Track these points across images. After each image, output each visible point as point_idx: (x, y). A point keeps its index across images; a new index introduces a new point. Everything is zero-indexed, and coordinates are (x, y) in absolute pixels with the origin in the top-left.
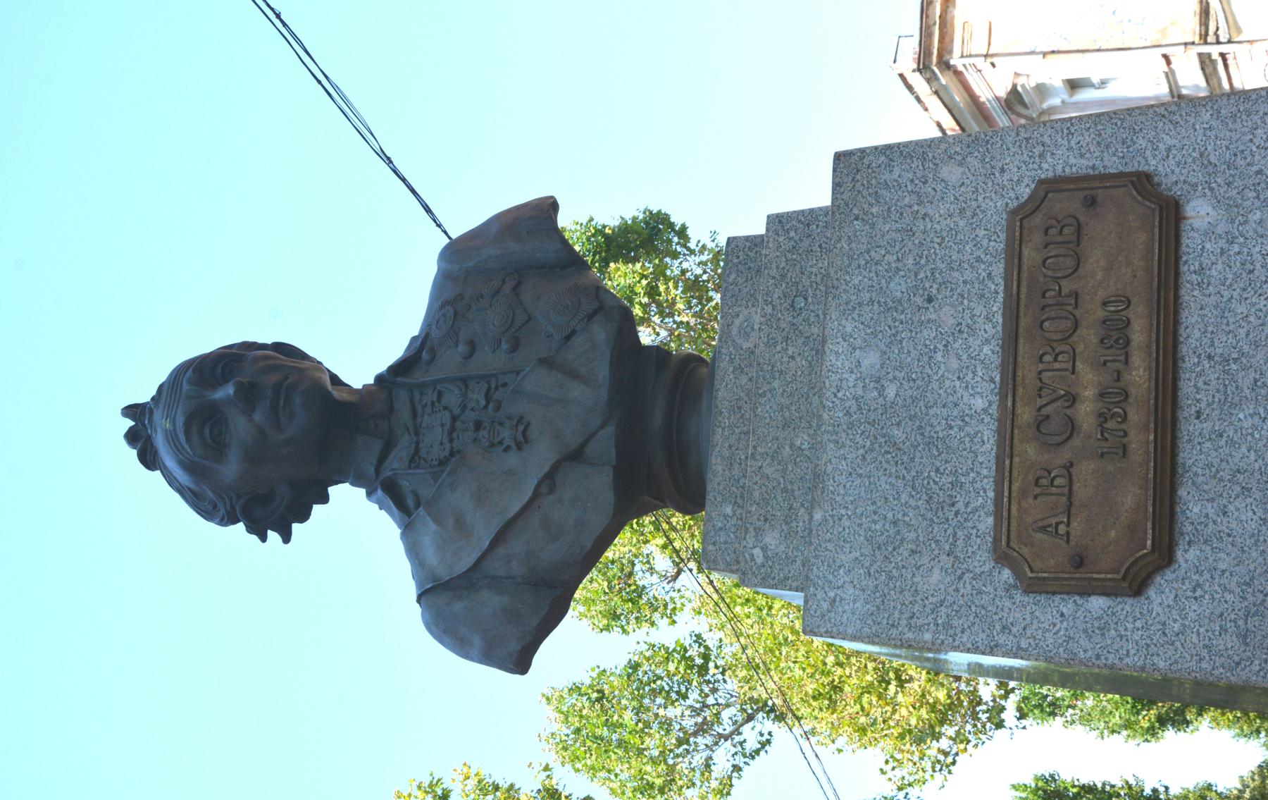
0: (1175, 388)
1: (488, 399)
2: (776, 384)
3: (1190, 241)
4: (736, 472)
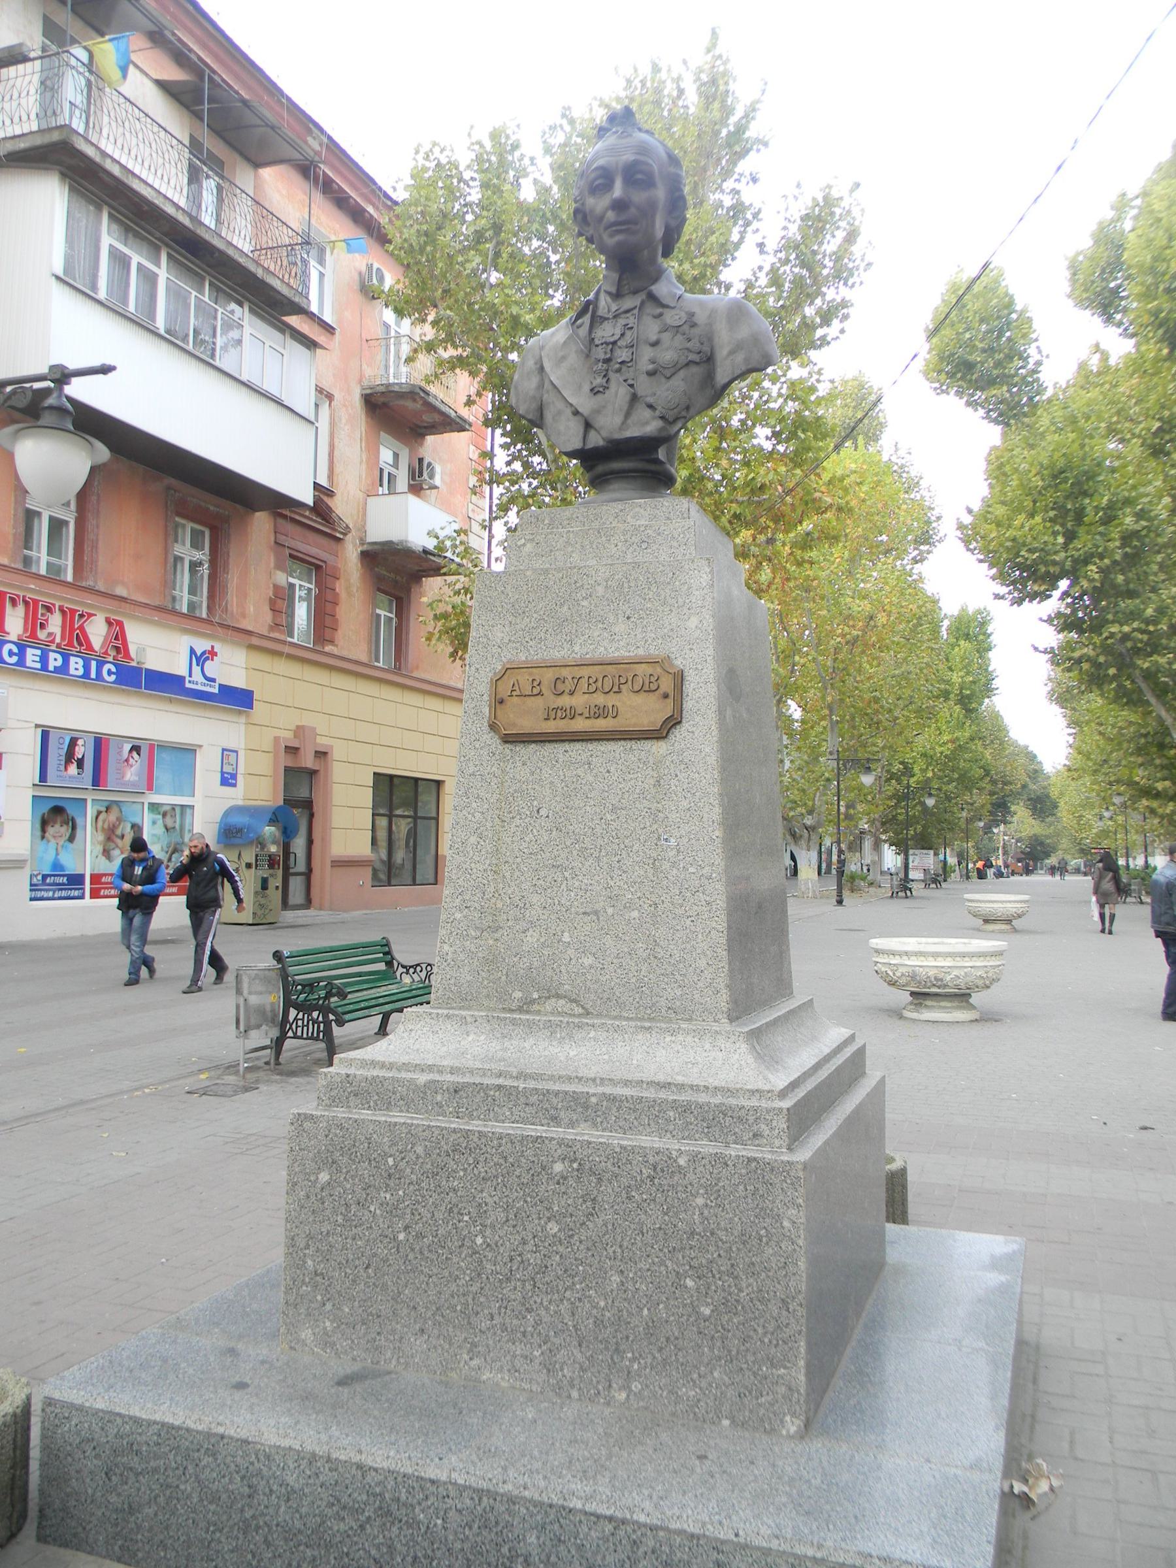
0: (578, 741)
1: (623, 363)
2: (604, 539)
3: (647, 744)
4: (566, 522)
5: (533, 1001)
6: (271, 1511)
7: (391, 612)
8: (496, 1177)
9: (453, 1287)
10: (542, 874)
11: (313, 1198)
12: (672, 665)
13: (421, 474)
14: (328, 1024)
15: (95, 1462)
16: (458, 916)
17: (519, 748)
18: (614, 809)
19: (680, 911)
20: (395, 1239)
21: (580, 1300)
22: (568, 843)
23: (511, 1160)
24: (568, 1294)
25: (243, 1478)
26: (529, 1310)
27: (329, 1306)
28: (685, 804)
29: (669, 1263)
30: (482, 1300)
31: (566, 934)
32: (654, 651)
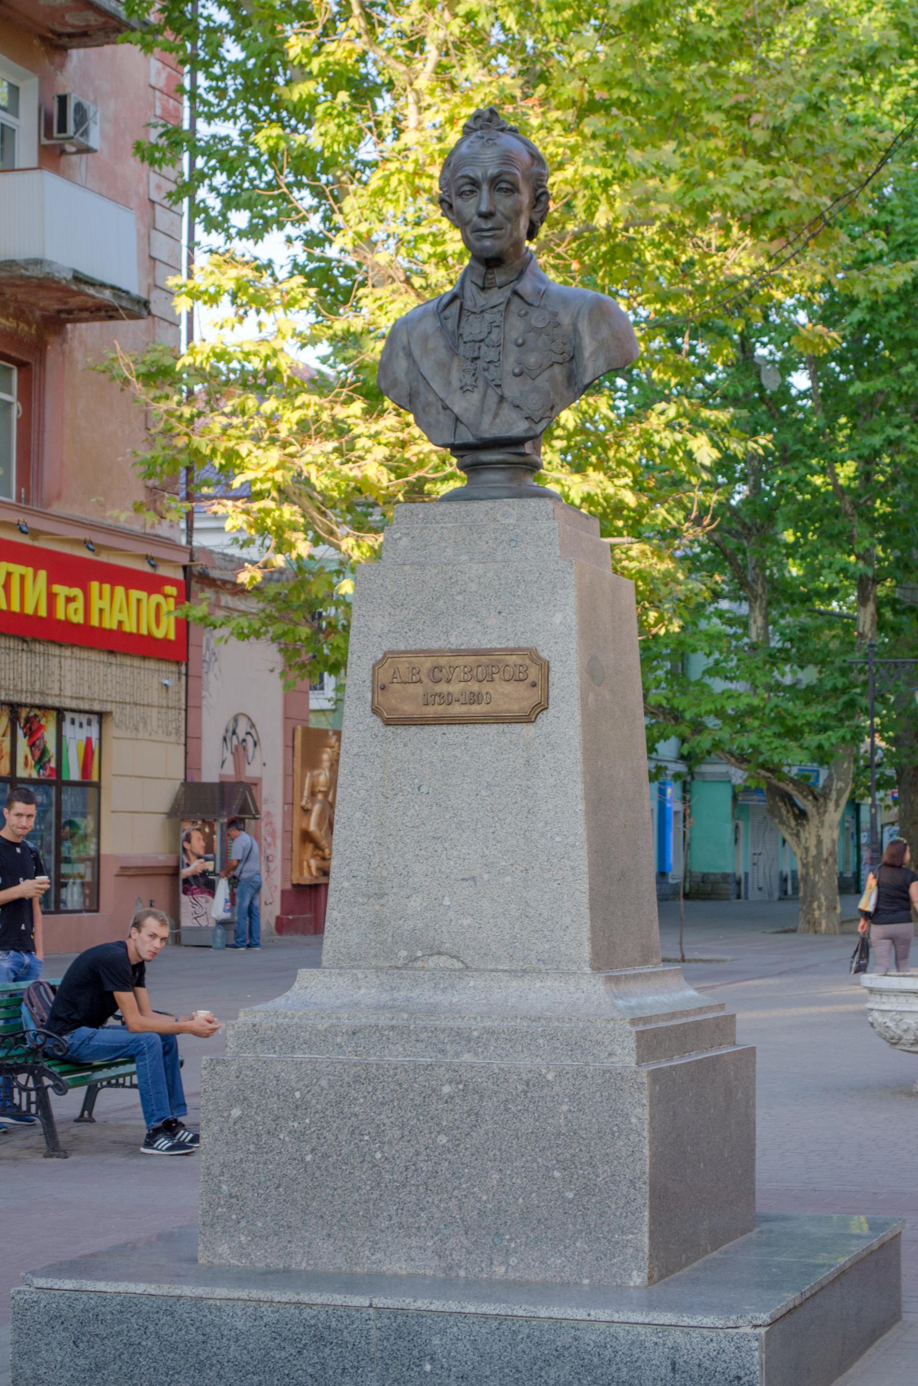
2: (475, 535)
3: (518, 727)
5: (417, 959)
6: (223, 1351)
7: (9, 392)
8: (392, 1101)
9: (356, 1196)
10: (424, 845)
11: (226, 1132)
12: (539, 657)
13: (63, 128)
14: (41, 1091)
15: (64, 1334)
16: (346, 884)
17: (400, 730)
18: (489, 786)
19: (547, 876)
20: (303, 1160)
21: (466, 1196)
22: (447, 817)
23: (405, 1086)
24: (456, 1193)
25: (197, 1329)
26: (422, 1209)
27: (243, 1223)
28: (552, 781)
29: (540, 1160)
30: (382, 1204)
31: (447, 898)
32: (523, 644)
